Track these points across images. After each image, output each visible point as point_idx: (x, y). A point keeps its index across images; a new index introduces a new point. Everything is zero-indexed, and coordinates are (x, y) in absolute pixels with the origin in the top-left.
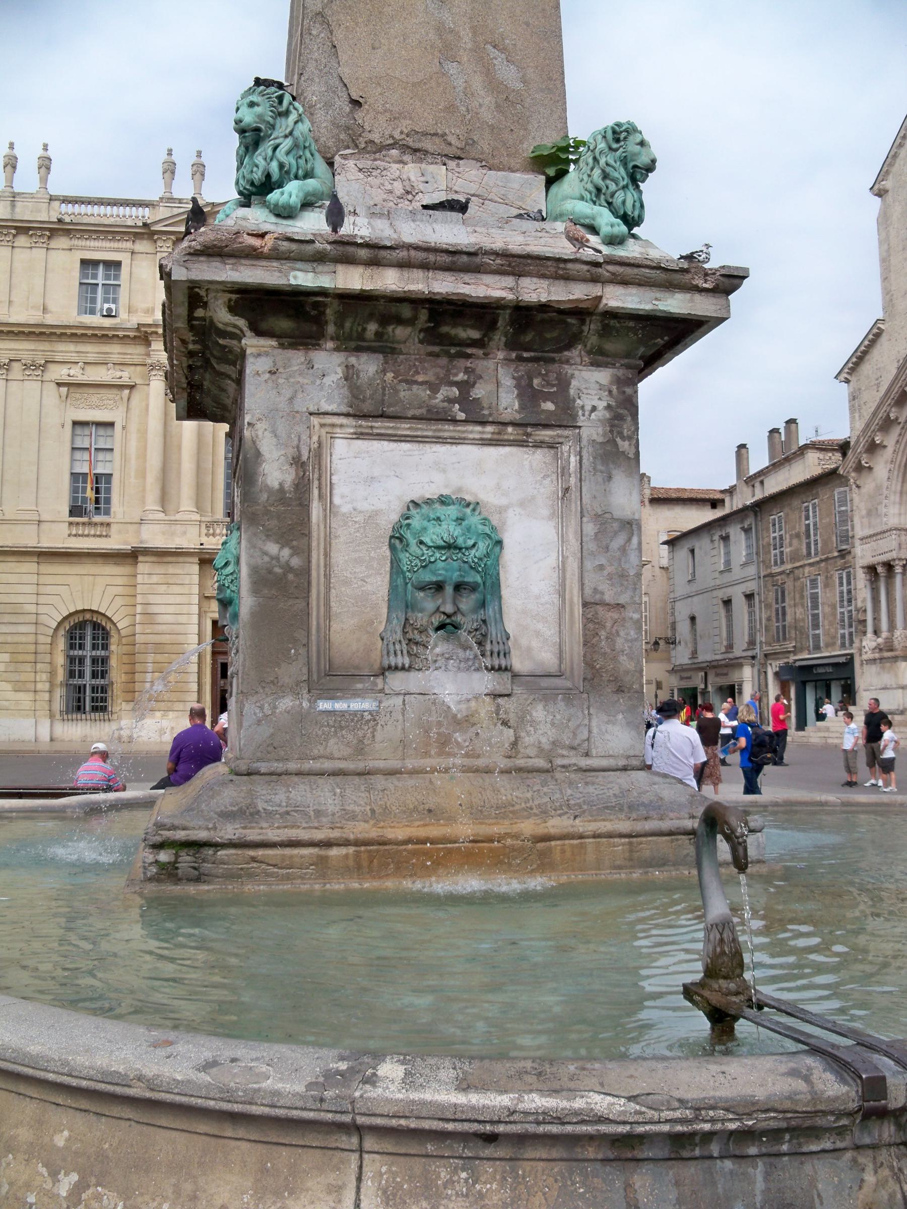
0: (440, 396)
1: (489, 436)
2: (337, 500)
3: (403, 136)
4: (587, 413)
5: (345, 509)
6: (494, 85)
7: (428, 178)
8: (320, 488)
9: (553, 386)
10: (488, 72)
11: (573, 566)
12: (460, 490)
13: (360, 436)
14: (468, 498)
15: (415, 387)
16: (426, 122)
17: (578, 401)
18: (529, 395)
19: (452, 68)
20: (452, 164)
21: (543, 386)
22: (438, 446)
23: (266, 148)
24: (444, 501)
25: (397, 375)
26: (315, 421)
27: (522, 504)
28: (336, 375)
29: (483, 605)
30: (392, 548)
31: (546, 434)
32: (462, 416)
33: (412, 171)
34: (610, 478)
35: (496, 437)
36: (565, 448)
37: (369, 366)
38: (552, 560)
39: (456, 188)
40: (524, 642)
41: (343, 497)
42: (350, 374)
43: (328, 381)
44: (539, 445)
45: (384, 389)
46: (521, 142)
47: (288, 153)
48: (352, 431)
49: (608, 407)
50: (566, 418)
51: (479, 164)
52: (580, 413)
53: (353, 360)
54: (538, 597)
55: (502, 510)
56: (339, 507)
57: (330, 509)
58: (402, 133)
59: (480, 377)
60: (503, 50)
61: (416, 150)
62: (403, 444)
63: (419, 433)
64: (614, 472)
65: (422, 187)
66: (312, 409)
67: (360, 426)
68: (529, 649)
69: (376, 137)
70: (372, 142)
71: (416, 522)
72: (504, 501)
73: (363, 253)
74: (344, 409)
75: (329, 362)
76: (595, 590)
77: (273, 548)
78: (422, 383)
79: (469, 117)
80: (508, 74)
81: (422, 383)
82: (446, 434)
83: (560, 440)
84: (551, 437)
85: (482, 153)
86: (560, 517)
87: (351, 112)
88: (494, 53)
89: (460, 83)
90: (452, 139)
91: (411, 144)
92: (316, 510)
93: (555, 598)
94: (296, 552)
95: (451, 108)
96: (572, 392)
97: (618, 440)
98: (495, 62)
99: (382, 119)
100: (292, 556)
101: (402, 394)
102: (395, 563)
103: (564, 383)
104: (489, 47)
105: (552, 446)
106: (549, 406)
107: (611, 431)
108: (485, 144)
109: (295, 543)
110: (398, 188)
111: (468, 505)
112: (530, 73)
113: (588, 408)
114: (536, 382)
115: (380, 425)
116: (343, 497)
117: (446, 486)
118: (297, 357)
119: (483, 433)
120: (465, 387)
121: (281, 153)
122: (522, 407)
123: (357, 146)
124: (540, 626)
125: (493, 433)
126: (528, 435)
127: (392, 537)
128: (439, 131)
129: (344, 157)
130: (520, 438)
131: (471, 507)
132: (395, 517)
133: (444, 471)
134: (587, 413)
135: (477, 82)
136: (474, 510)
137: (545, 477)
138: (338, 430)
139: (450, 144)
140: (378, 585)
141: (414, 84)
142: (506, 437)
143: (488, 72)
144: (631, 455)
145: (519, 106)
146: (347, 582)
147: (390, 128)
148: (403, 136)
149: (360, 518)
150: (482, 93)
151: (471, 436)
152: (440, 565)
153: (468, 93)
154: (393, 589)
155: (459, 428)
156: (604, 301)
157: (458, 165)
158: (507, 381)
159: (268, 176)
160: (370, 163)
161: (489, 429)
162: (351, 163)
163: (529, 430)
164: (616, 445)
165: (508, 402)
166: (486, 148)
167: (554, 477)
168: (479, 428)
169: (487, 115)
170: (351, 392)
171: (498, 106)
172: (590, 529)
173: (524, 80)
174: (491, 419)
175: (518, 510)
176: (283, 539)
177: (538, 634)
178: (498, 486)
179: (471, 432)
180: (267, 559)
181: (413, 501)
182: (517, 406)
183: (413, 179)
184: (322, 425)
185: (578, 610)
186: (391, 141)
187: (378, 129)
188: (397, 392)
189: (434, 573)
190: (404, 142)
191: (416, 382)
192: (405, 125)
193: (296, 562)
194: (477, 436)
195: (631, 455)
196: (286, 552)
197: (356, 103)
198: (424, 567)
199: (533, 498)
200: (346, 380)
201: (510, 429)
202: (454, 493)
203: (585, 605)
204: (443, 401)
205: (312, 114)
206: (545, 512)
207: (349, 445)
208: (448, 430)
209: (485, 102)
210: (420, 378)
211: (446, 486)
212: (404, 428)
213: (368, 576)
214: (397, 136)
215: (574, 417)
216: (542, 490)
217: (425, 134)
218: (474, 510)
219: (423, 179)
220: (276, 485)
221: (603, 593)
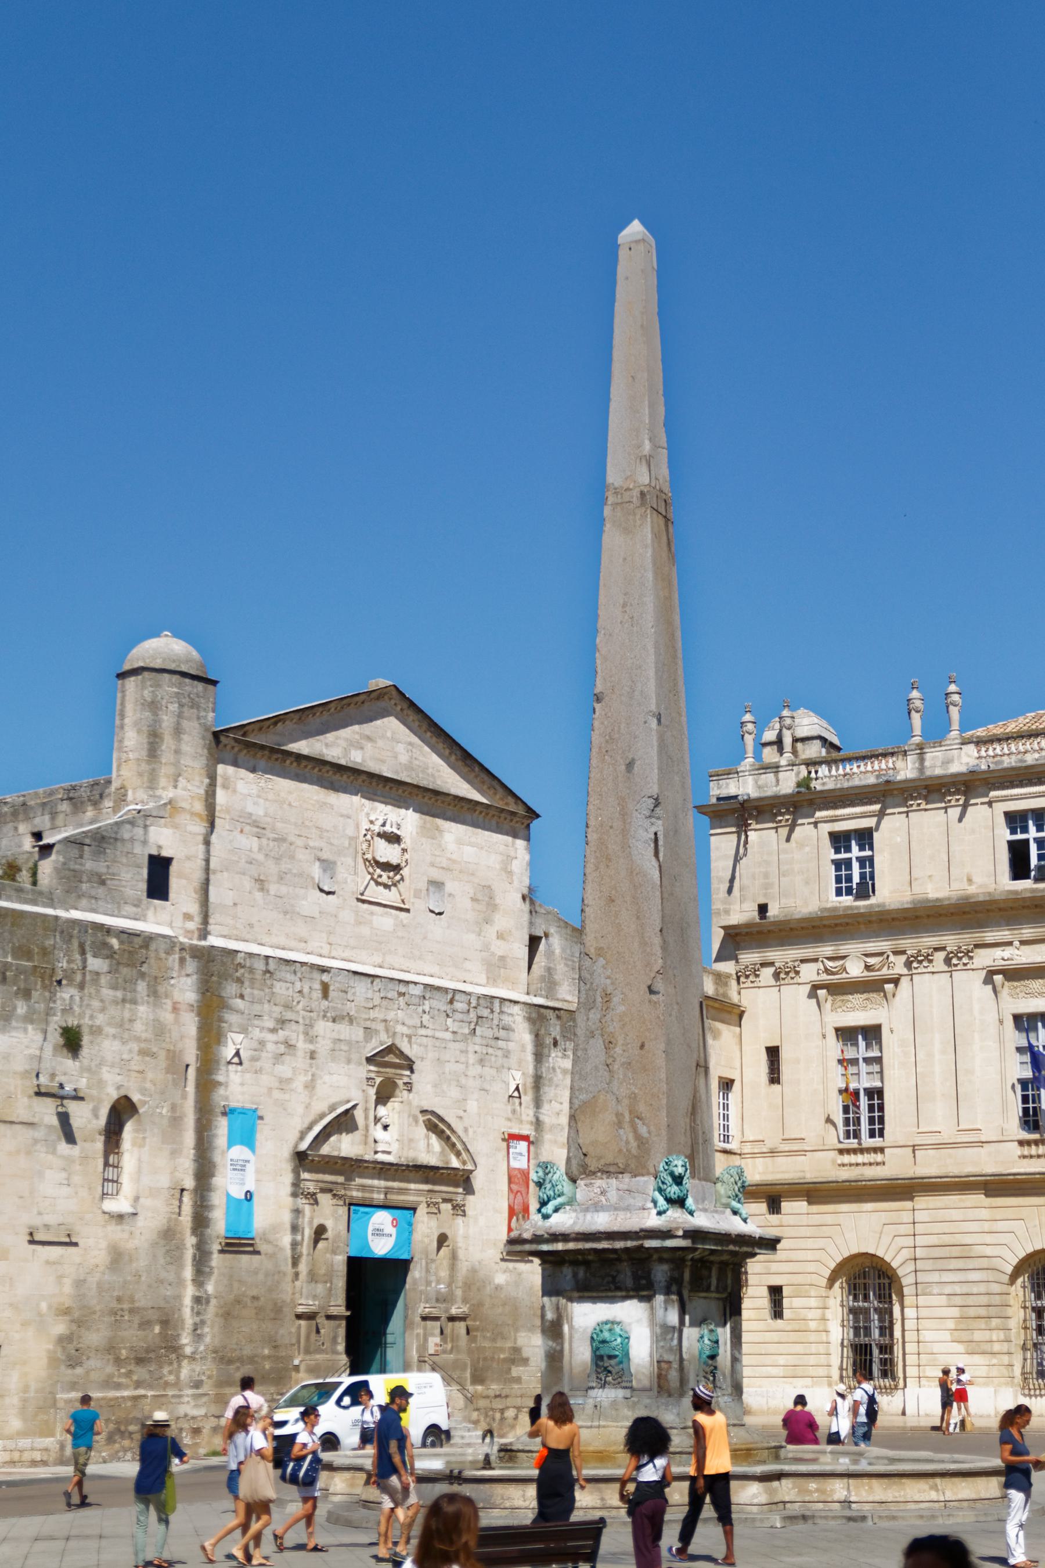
6: (638, 1137)
10: (635, 1131)
18: (636, 1277)
19: (621, 1132)
20: (620, 1176)
28: (569, 1276)
42: (575, 1275)
55: (630, 1324)
57: (571, 1327)
69: (592, 1169)
80: (643, 1130)
92: (566, 1328)
94: (558, 1344)
103: (649, 1273)
110: (598, 1190)
112: (652, 1128)
120: (614, 1278)
135: (631, 1137)
143: (635, 1131)
153: (627, 1142)
158: (629, 1274)
165: (629, 1282)
169: (634, 1151)
173: (649, 1132)
192: (602, 1162)
197: (585, 1155)
209: (634, 1144)
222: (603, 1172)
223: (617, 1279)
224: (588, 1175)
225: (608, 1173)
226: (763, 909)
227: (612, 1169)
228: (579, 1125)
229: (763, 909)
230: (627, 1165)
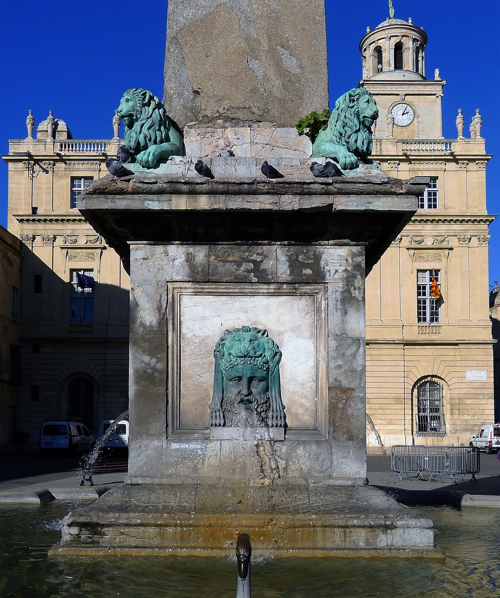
0: (242, 269)
1: (273, 291)
2: (184, 330)
3: (225, 111)
4: (332, 275)
5: (189, 335)
6: (282, 73)
7: (240, 136)
8: (173, 324)
9: (311, 259)
11: (323, 365)
12: (255, 323)
13: (196, 293)
14: (260, 327)
15: (227, 264)
16: (239, 99)
17: (326, 267)
18: (295, 265)
19: (254, 64)
20: (255, 125)
21: (305, 260)
22: (243, 297)
23: (137, 126)
24: (246, 330)
25: (217, 257)
26: (170, 286)
27: (293, 330)
28: (181, 260)
29: (267, 389)
30: (215, 356)
31: (307, 288)
32: (255, 280)
33: (230, 133)
34: (346, 313)
35: (276, 291)
36: (319, 296)
37: (200, 253)
38: (311, 362)
39: (255, 141)
40: (294, 410)
41: (187, 329)
42: (190, 259)
43: (177, 262)
44: (303, 295)
45: (209, 266)
46: (298, 108)
47: (149, 128)
48: (192, 291)
49: (346, 270)
50: (318, 278)
51: (272, 124)
52: (328, 274)
53: (191, 249)
54: (303, 384)
55: (280, 334)
56: (185, 334)
57: (179, 336)
58: (224, 109)
59: (267, 256)
60: (289, 48)
61: (233, 119)
62: (222, 297)
63: (231, 291)
64: (349, 309)
65: (235, 142)
66: (168, 279)
67: (196, 288)
68: (297, 414)
69: (208, 113)
70: (206, 116)
71: (227, 343)
72: (282, 329)
73: (185, 188)
74: (187, 279)
75: (177, 252)
76: (336, 380)
77: (146, 359)
78: (232, 262)
79: (265, 95)
80: (291, 64)
81: (232, 262)
82: (247, 291)
83: (316, 291)
84: (310, 289)
85: (274, 117)
86: (316, 336)
87: (194, 98)
88: (281, 50)
89: (260, 73)
90: (255, 110)
91: (230, 115)
93: (313, 385)
94: (159, 360)
95: (254, 90)
96: (322, 262)
97: (352, 289)
98: (282, 57)
99: (212, 101)
100: (157, 362)
101: (220, 268)
102: (217, 366)
103: (318, 258)
104: (279, 47)
105: (311, 295)
106: (309, 271)
107: (347, 285)
108: (275, 112)
109: (159, 356)
111: (259, 332)
112: (305, 62)
113: (332, 272)
114: (300, 258)
115: (207, 287)
116: (187, 329)
117: (248, 321)
118: (159, 249)
119: (269, 289)
121: (145, 129)
122: (292, 273)
123: (197, 120)
124: (303, 401)
125: (275, 289)
126: (295, 289)
127: (215, 351)
128: (247, 106)
129: (190, 127)
130: (291, 291)
131: (261, 333)
132: (217, 340)
133: (246, 312)
134: (332, 275)
135: (271, 73)
136: (263, 334)
137: (306, 314)
138: (184, 290)
139: (254, 113)
140: (208, 378)
141: (231, 77)
142: (283, 291)
143: (278, 64)
144: (360, 299)
145: (297, 84)
146: (190, 377)
147: (217, 106)
148: (225, 111)
149: (197, 340)
150: (274, 78)
151: (262, 291)
152: (240, 366)
154: (216, 379)
155: (254, 287)
156: (334, 207)
157: (259, 126)
158: (283, 258)
159: (138, 143)
160: (204, 129)
161: (272, 286)
162: (193, 131)
163: (297, 285)
164: (350, 292)
165: (283, 270)
166: (276, 114)
167: (313, 313)
168: (266, 286)
169: (277, 93)
170: (190, 269)
171: (284, 86)
172: (333, 344)
174: (272, 281)
175: (290, 333)
176: (152, 353)
177: (302, 405)
178: (279, 320)
179: (262, 289)
180: (143, 365)
181: (227, 330)
182: (288, 272)
183: (230, 137)
184: (174, 288)
185: (326, 392)
186: (218, 115)
187: (209, 108)
188: (217, 267)
189: (237, 371)
190: (226, 115)
191: (228, 261)
192: (226, 104)
193: (160, 366)
194: (265, 291)
195: (360, 299)
196: (154, 360)
197: (196, 92)
198: (232, 368)
199: (299, 327)
200: (187, 262)
201: (285, 286)
202: (251, 325)
203: (329, 389)
204: (244, 272)
205: (171, 102)
206: (307, 334)
207: (191, 299)
208: (248, 288)
209: (276, 84)
210: (231, 259)
211: (248, 321)
212: (222, 288)
213: (202, 373)
214: (222, 111)
215: (324, 278)
216: (305, 322)
217: (238, 108)
218: (263, 334)
219: (237, 137)
220: (148, 324)
221: (341, 382)
222: (228, 119)
223: (263, 266)
224: (200, 122)
225: (235, 121)
226: (34, 210)
227: (240, 115)
228: (186, 50)
229: (34, 210)
230: (266, 111)
